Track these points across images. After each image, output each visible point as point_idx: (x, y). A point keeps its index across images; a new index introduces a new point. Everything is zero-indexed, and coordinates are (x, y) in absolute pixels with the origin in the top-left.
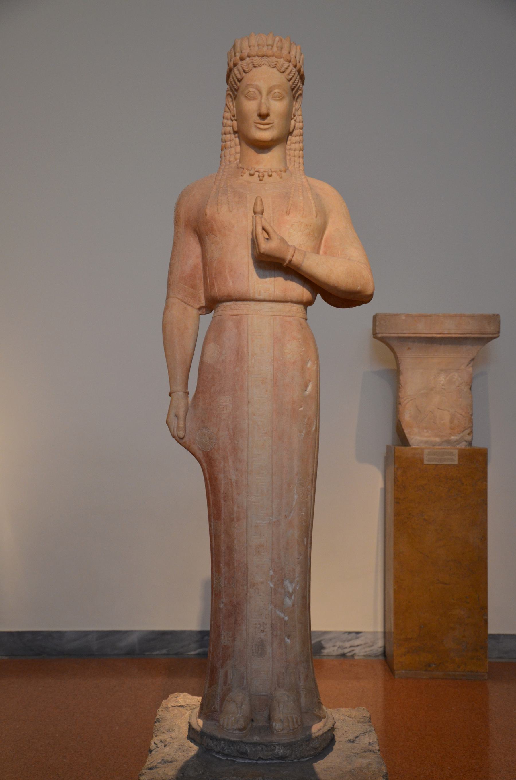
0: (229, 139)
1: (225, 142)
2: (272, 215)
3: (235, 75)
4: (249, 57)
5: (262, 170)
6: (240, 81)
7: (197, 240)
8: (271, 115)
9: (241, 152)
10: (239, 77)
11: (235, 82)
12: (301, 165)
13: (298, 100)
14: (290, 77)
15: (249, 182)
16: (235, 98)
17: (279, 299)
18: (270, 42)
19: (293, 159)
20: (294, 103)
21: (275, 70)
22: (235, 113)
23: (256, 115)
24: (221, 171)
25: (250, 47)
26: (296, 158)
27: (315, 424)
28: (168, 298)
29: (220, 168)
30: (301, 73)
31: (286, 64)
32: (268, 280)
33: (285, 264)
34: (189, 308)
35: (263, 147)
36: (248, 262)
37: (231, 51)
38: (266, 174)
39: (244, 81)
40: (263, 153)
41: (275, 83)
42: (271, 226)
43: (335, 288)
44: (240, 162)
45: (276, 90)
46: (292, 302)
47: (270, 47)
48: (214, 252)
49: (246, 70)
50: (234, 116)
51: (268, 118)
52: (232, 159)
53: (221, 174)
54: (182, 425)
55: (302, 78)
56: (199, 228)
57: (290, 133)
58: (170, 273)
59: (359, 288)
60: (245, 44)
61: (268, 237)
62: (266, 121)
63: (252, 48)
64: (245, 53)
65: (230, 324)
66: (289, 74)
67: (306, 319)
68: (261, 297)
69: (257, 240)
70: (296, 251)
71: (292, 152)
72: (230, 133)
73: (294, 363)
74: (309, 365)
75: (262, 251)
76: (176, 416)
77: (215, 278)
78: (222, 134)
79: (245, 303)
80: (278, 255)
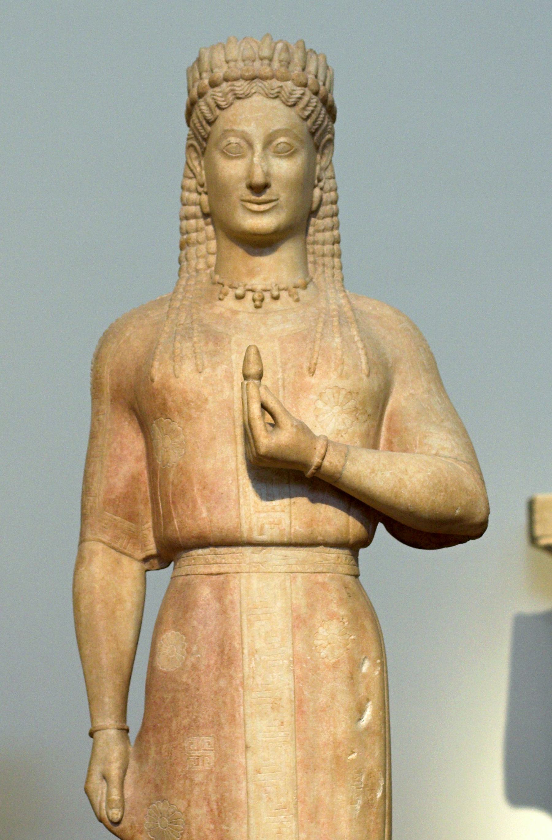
0: (194, 227)
1: (188, 233)
2: (280, 376)
3: (202, 113)
4: (226, 80)
5: (259, 287)
6: (210, 123)
7: (136, 425)
8: (273, 185)
9: (218, 252)
10: (209, 116)
11: (202, 126)
12: (337, 272)
13: (326, 151)
14: (307, 113)
15: (235, 312)
16: (203, 153)
17: (300, 541)
18: (266, 52)
19: (320, 261)
20: (318, 157)
21: (277, 102)
22: (204, 178)
23: (243, 185)
24: (181, 290)
25: (227, 62)
26: (327, 260)
27: (382, 784)
28: (82, 540)
29: (178, 283)
30: (329, 103)
31: (299, 91)
32: (276, 503)
33: (309, 473)
34: (125, 560)
35: (260, 244)
36: (237, 470)
37: (193, 67)
38: (267, 295)
39: (220, 125)
40: (261, 254)
41: (278, 127)
42: (279, 402)
43: (410, 514)
44: (216, 271)
45: (282, 139)
46: (327, 544)
47: (266, 62)
48: (171, 452)
49: (223, 104)
50: (202, 186)
51: (268, 191)
52: (201, 266)
53: (180, 296)
54: (115, 795)
55: (331, 112)
56: (139, 403)
57: (313, 213)
58: (86, 492)
59: (457, 511)
60: (219, 57)
61: (273, 422)
62: (263, 197)
63: (232, 64)
64: (219, 73)
65: (205, 592)
66: (304, 109)
67: (357, 576)
68: (265, 538)
69: (251, 430)
70: (330, 448)
71: (317, 247)
72: (195, 217)
73: (335, 666)
74: (365, 669)
75: (263, 450)
76: (105, 777)
77: (174, 502)
78: (181, 219)
79: (234, 549)
80: (294, 457)
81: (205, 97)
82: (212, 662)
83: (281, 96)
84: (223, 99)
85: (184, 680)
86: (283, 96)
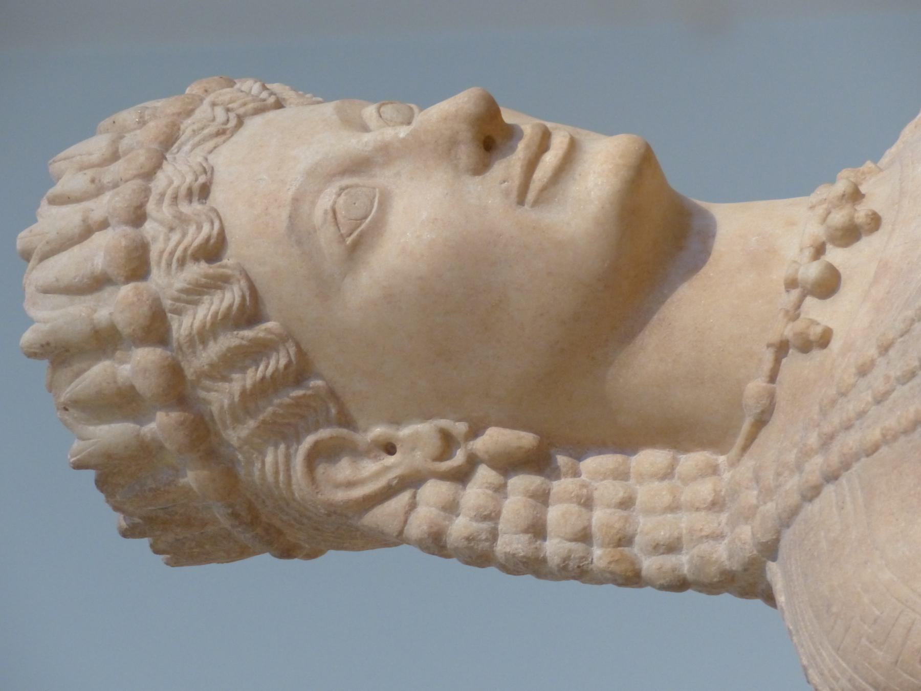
0: (574, 508)
1: (585, 537)
4: (138, 217)
6: (250, 313)
52: (705, 489)
72: (542, 498)
81: (167, 303)
83: (241, 111)
84: (192, 230)
86: (245, 104)
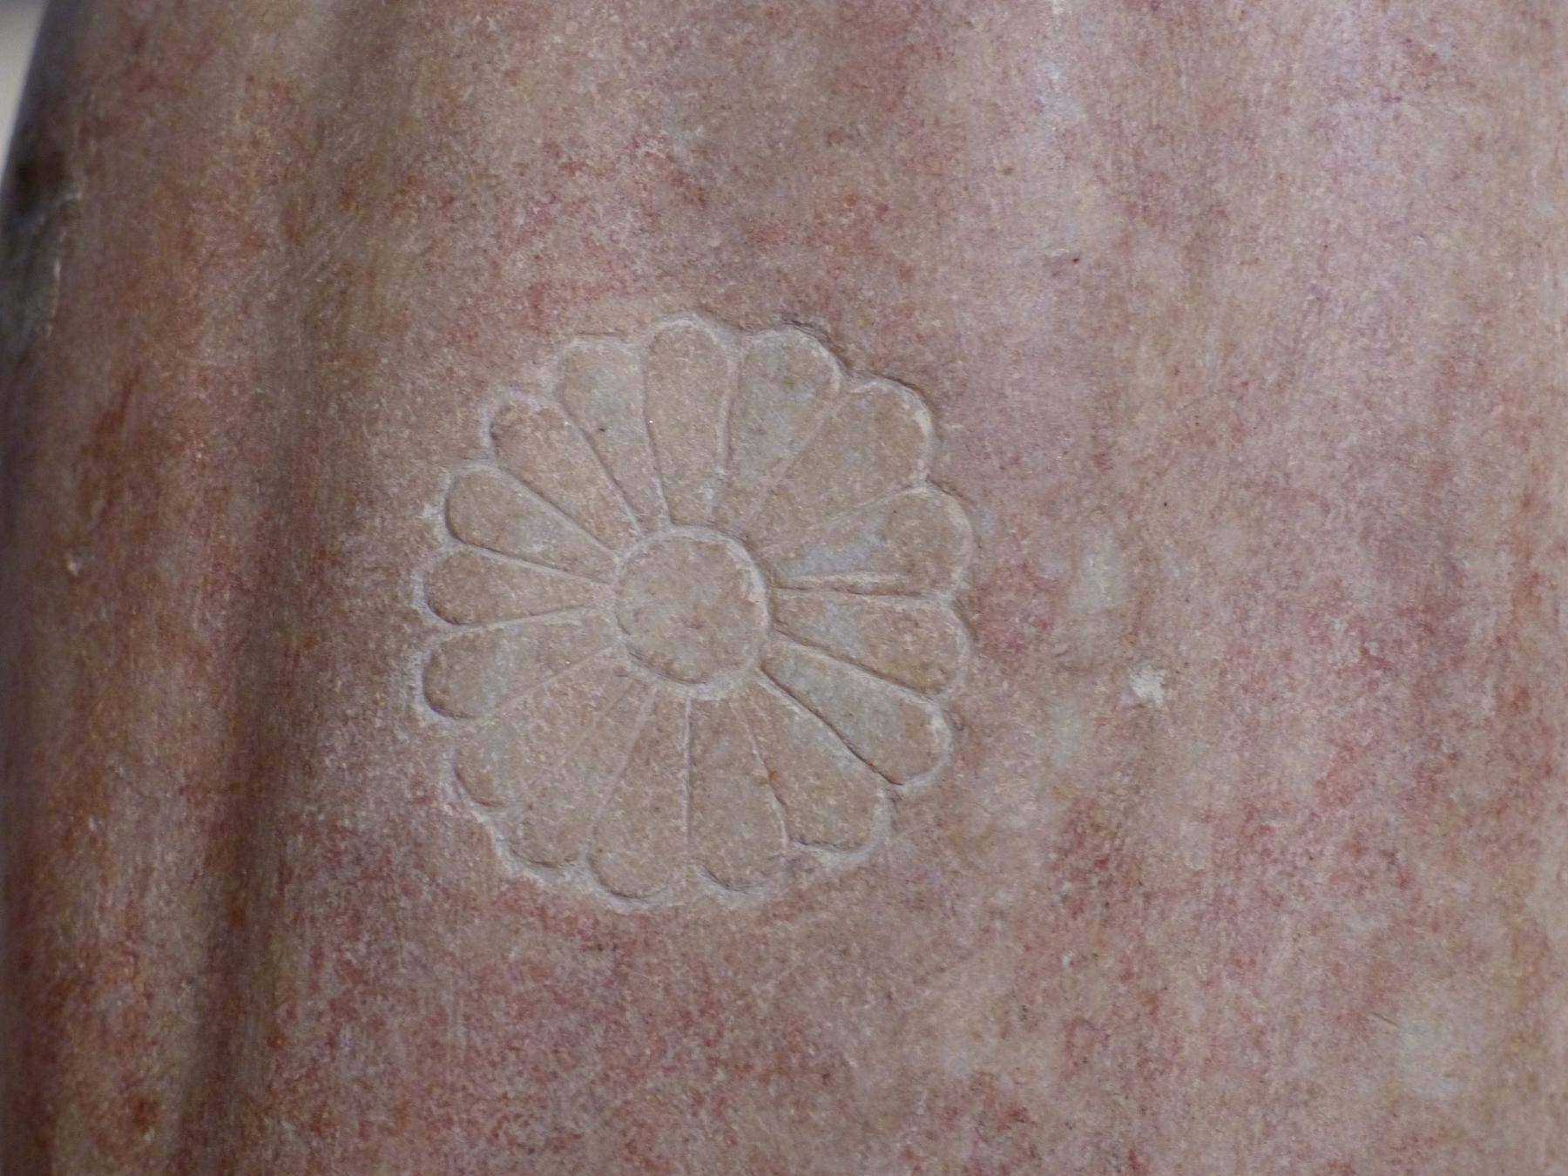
82: (1299, 765)
85: (957, 1060)
